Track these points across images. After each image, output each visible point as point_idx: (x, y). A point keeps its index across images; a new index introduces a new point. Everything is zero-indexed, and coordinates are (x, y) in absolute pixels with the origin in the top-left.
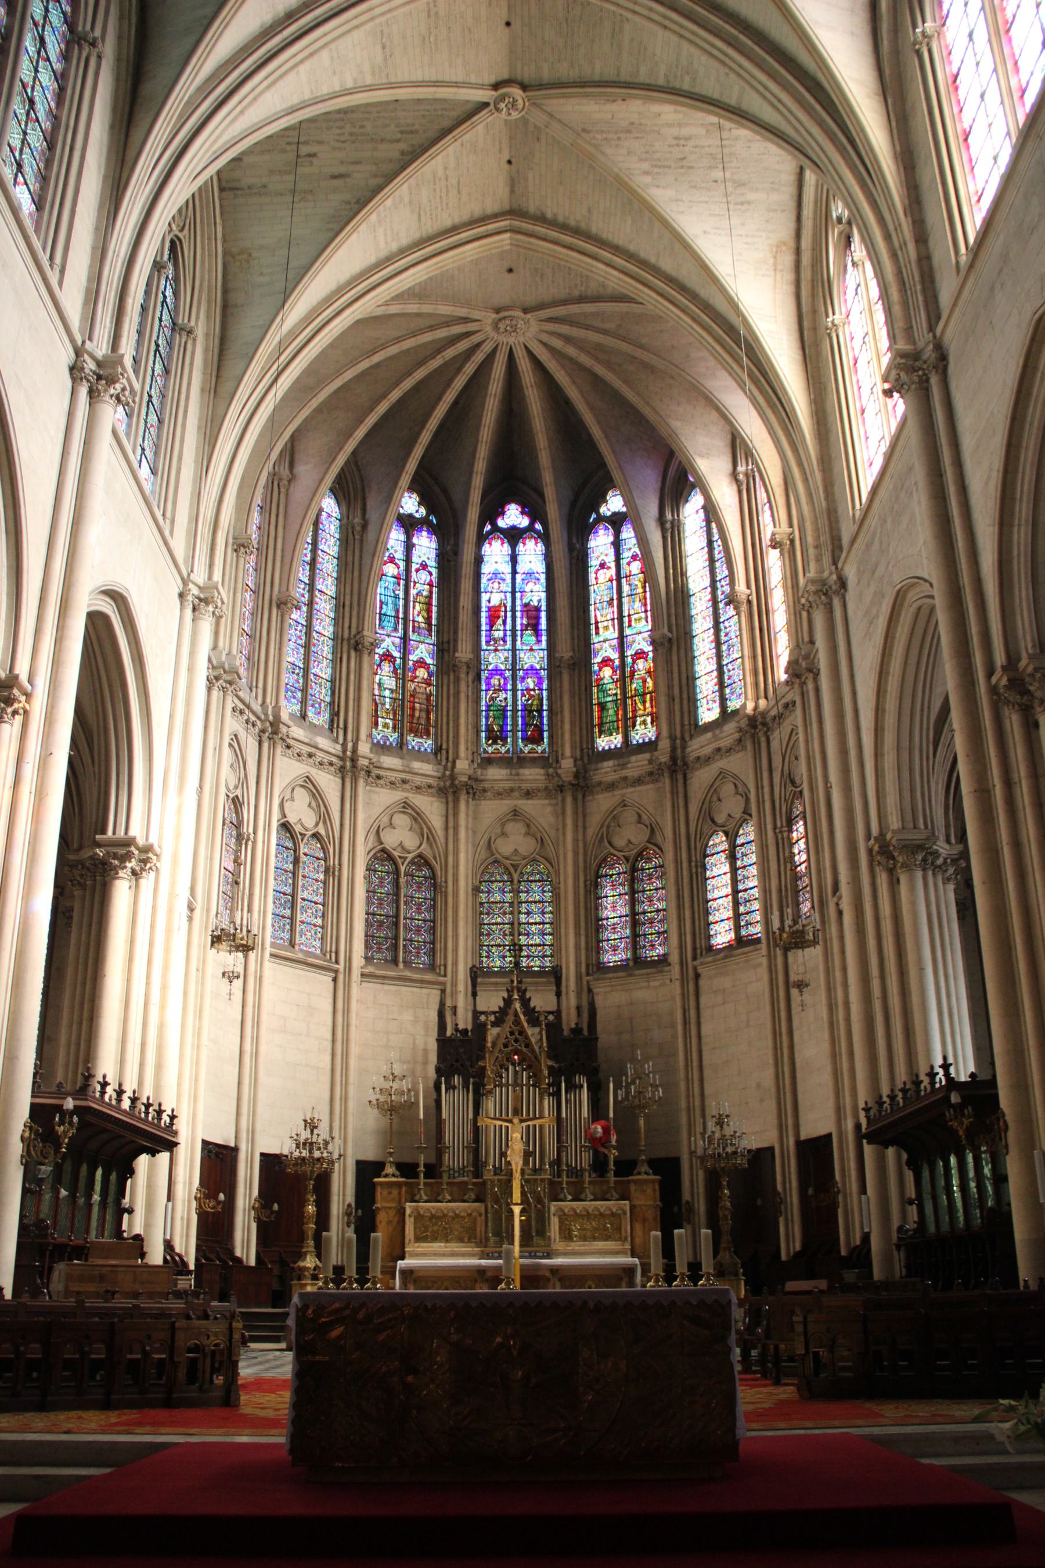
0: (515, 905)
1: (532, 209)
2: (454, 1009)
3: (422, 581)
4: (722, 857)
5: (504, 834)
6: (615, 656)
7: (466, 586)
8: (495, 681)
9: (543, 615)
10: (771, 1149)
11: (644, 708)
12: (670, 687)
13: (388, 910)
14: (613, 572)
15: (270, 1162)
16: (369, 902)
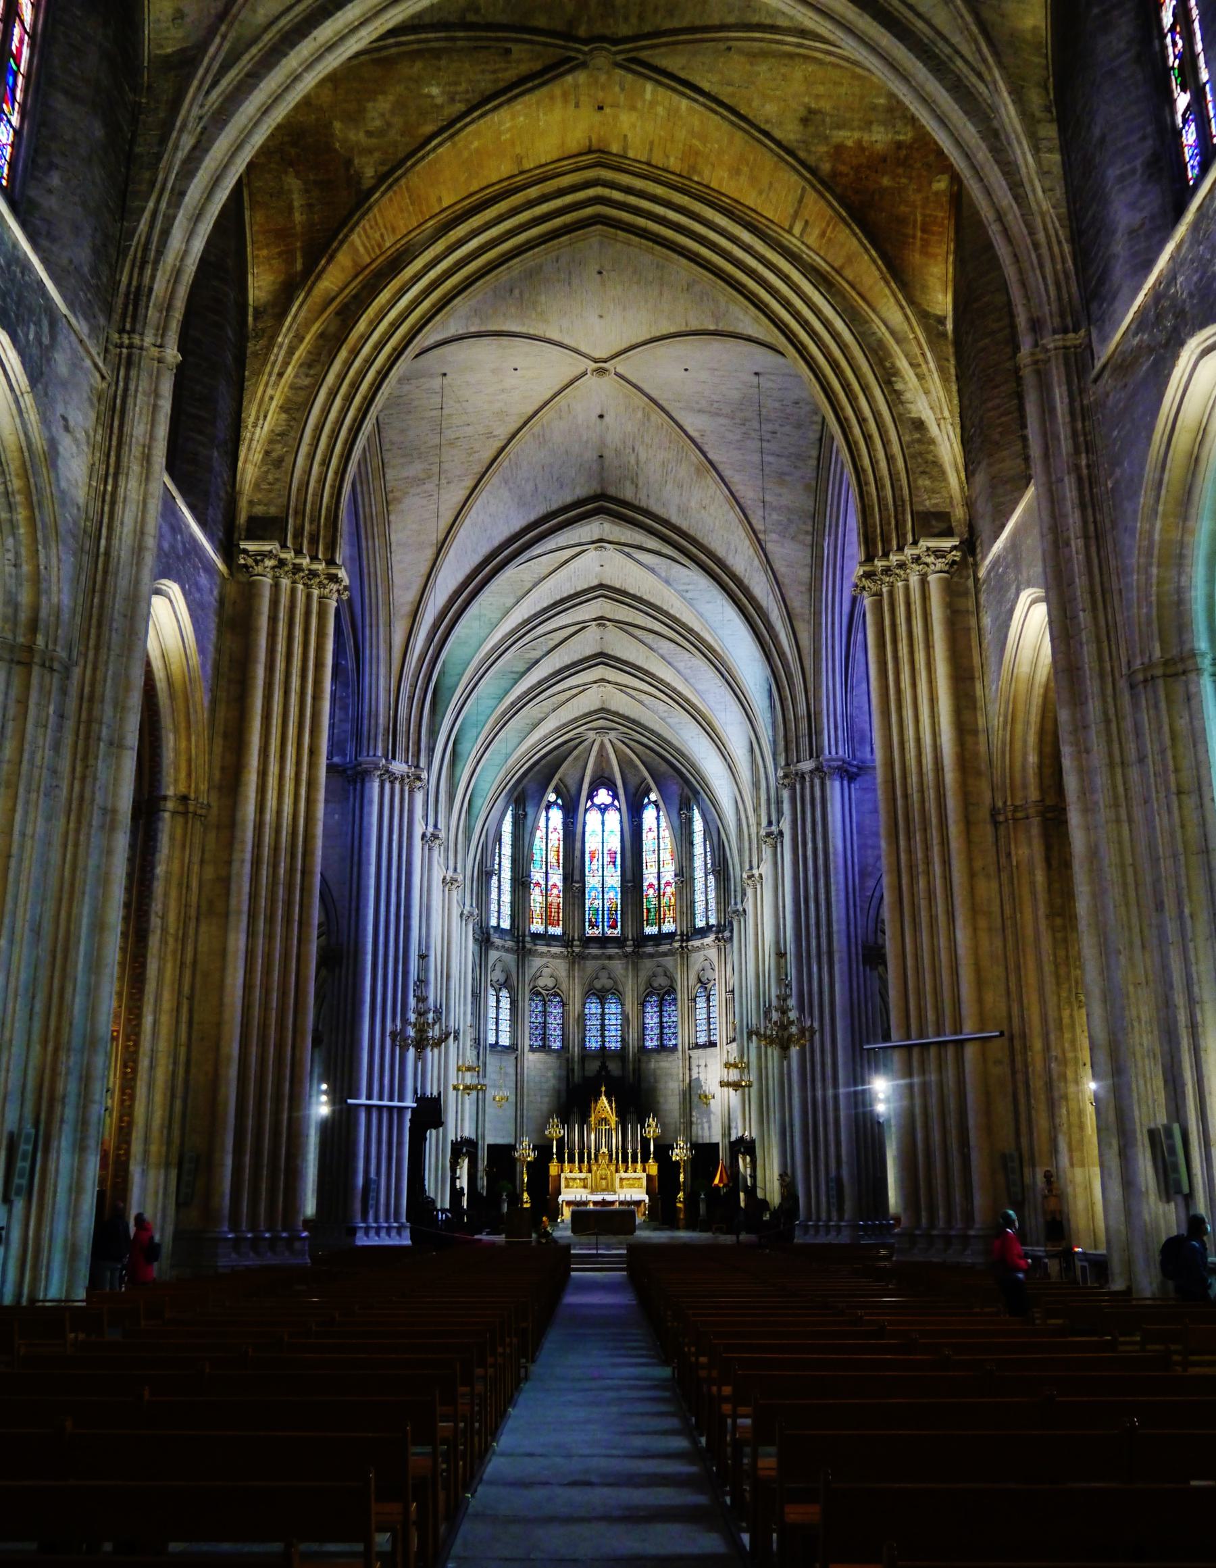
0: (603, 1014)
1: (613, 708)
2: (573, 1070)
3: (556, 838)
4: (704, 999)
5: (597, 978)
6: (655, 883)
7: (578, 845)
8: (593, 894)
9: (619, 856)
10: (718, 1144)
11: (670, 914)
12: (681, 907)
13: (540, 1020)
14: (655, 834)
15: (491, 1147)
16: (531, 1016)
